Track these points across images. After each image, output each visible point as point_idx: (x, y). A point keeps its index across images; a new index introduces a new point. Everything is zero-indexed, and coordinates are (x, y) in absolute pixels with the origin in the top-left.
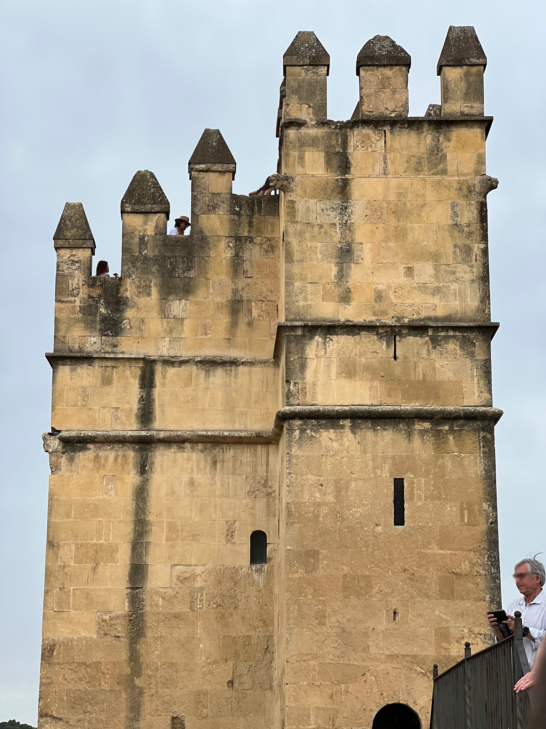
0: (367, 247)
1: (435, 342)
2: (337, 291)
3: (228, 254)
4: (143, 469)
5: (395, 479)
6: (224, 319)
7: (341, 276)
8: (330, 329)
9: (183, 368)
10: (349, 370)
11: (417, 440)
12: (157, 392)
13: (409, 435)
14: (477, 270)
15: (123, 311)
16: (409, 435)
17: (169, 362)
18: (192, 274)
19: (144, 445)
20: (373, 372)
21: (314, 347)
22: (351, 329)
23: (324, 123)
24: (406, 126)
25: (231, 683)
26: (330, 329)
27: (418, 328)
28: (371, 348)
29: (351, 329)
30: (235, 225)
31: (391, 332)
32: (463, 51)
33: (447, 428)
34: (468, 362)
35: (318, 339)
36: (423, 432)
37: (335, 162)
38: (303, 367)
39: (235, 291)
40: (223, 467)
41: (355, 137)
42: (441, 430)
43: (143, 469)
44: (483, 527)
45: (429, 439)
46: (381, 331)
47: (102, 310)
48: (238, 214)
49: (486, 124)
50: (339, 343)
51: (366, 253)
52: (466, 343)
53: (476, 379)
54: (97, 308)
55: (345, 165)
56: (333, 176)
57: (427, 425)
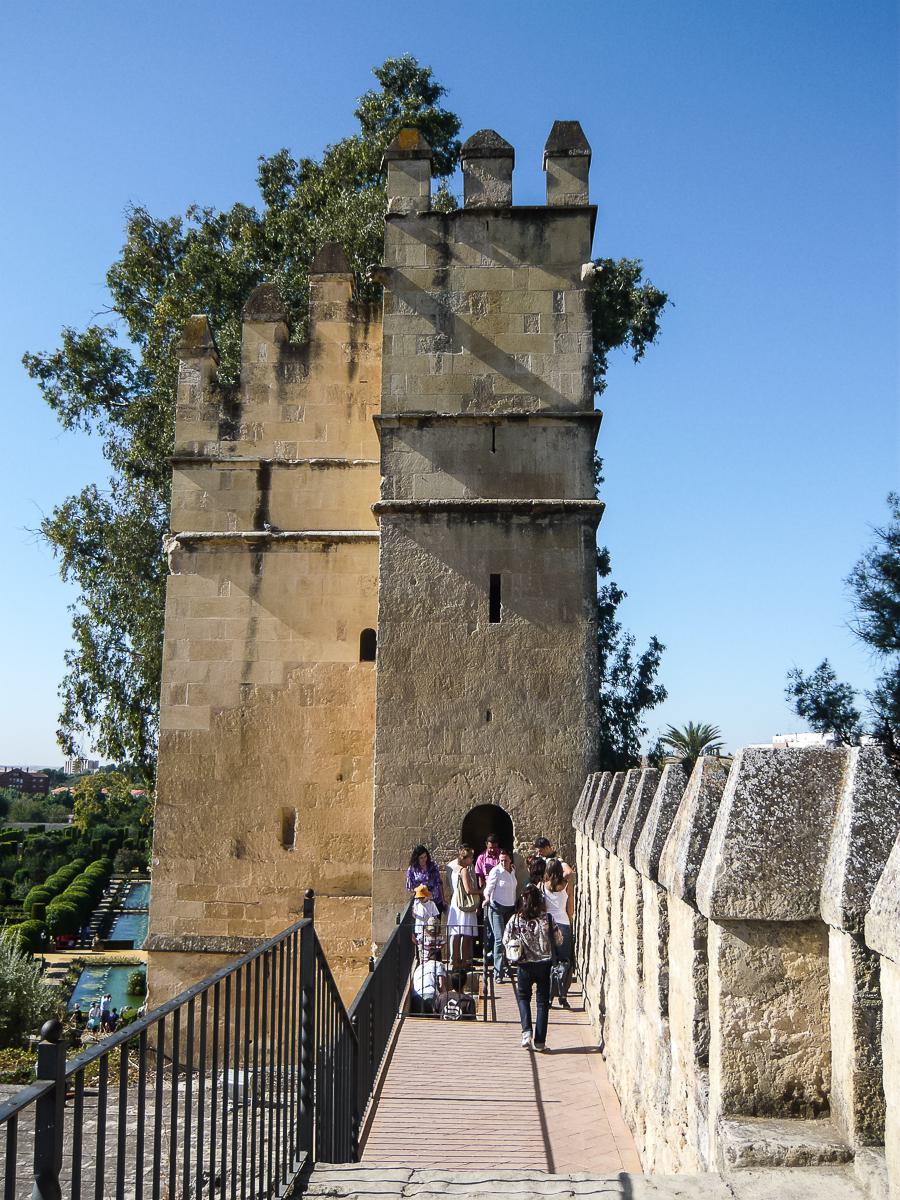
4: (257, 568)
5: (491, 575)
9: (298, 469)
11: (515, 535)
12: (271, 493)
13: (507, 529)
15: (239, 417)
16: (507, 529)
17: (281, 464)
19: (260, 546)
24: (509, 216)
25: (341, 778)
32: (568, 145)
33: (547, 521)
36: (521, 526)
40: (334, 566)
42: (541, 525)
43: (257, 568)
46: (479, 422)
47: (221, 415)
48: (354, 321)
49: (591, 212)
53: (578, 472)
54: (218, 413)
57: (526, 519)
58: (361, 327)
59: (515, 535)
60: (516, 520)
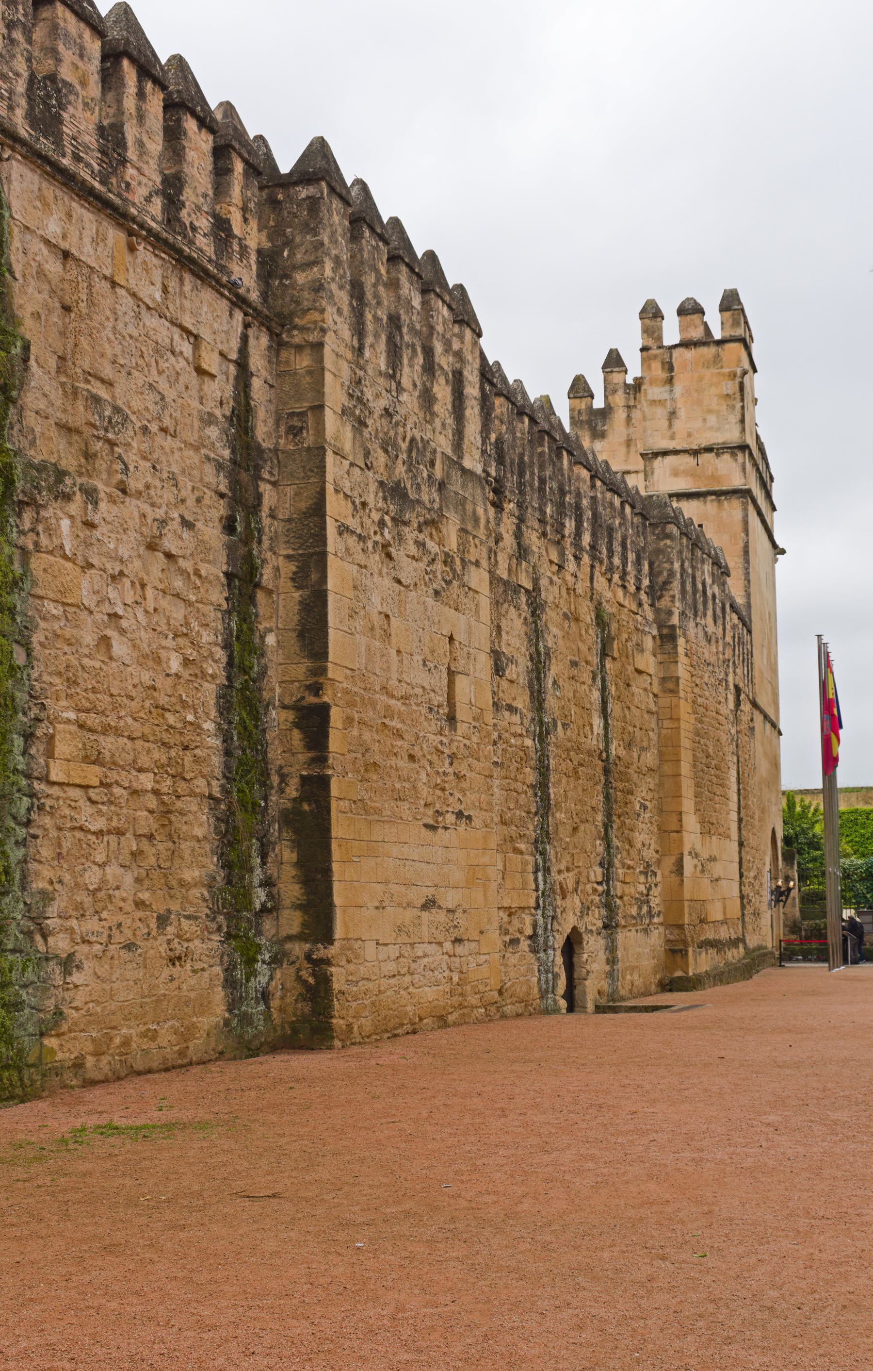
0: (683, 410)
1: (718, 455)
2: (669, 434)
3: (624, 415)
6: (623, 450)
7: (670, 426)
8: (665, 453)
10: (675, 473)
11: (709, 505)
13: (705, 502)
14: (739, 417)
16: (705, 502)
18: (605, 428)
20: (688, 473)
21: (658, 462)
22: (676, 452)
23: (661, 347)
26: (665, 453)
27: (709, 449)
28: (688, 461)
29: (676, 452)
30: (628, 399)
31: (695, 453)
34: (734, 464)
35: (660, 458)
36: (712, 501)
37: (667, 366)
38: (652, 473)
39: (628, 435)
41: (676, 353)
44: (742, 545)
45: (715, 504)
50: (670, 459)
51: (682, 413)
52: (733, 455)
55: (671, 369)
56: (665, 375)
57: (714, 497)
58: (632, 396)
59: (709, 505)
60: (709, 498)
